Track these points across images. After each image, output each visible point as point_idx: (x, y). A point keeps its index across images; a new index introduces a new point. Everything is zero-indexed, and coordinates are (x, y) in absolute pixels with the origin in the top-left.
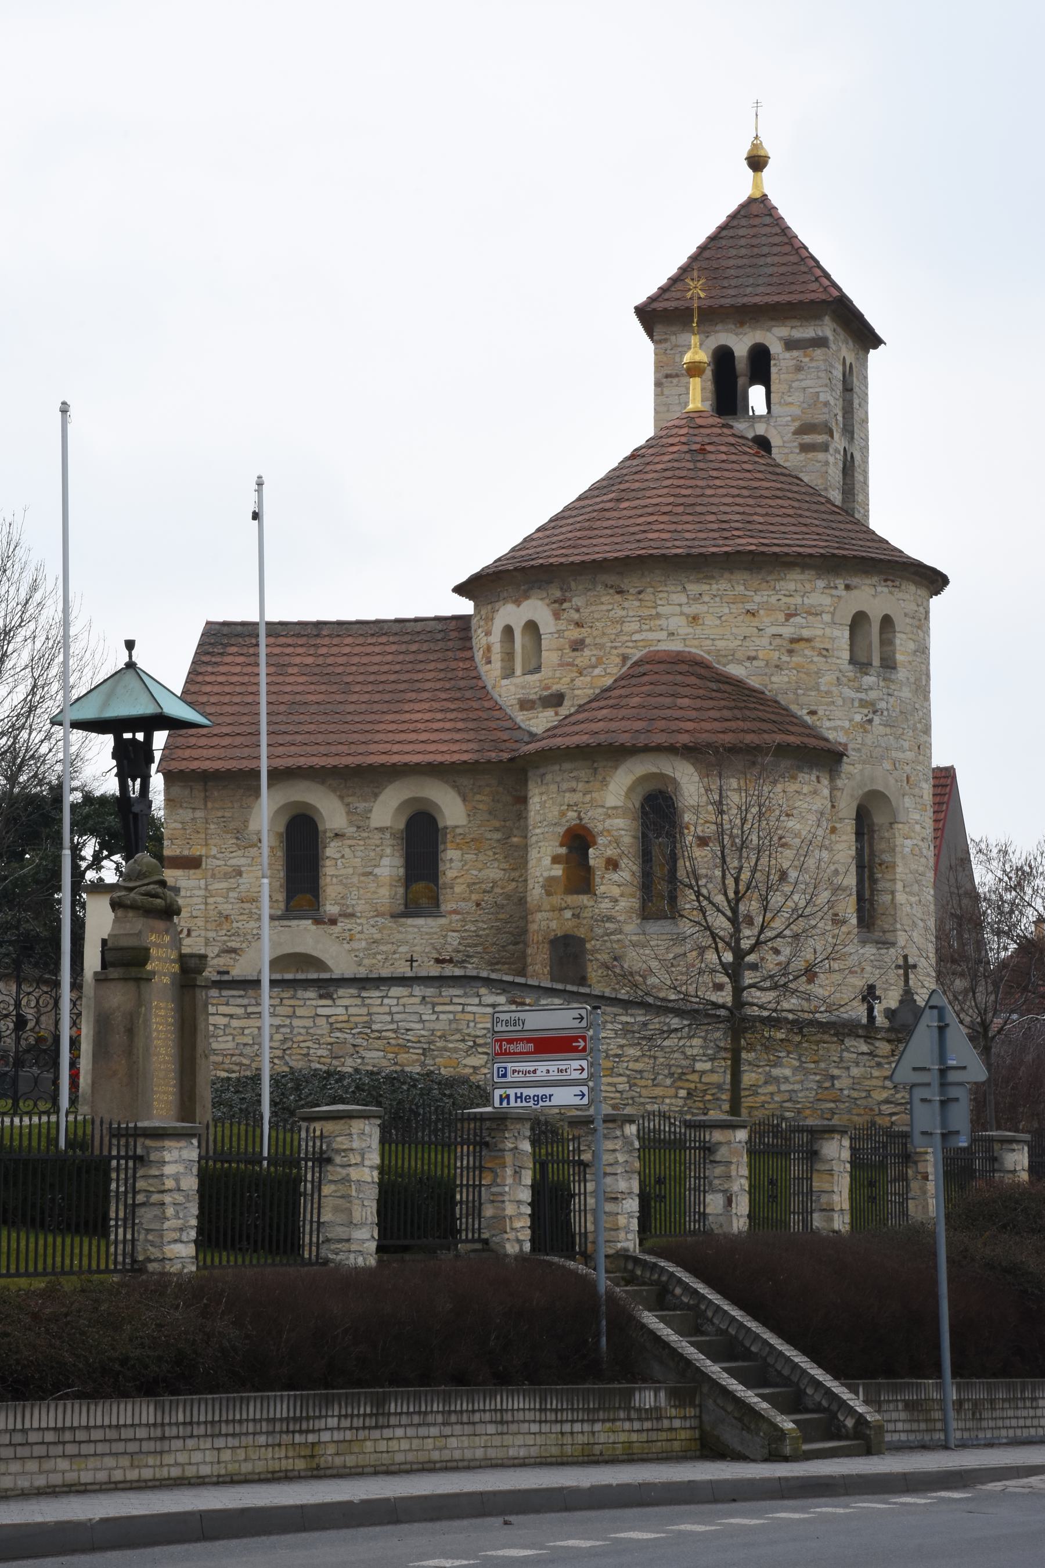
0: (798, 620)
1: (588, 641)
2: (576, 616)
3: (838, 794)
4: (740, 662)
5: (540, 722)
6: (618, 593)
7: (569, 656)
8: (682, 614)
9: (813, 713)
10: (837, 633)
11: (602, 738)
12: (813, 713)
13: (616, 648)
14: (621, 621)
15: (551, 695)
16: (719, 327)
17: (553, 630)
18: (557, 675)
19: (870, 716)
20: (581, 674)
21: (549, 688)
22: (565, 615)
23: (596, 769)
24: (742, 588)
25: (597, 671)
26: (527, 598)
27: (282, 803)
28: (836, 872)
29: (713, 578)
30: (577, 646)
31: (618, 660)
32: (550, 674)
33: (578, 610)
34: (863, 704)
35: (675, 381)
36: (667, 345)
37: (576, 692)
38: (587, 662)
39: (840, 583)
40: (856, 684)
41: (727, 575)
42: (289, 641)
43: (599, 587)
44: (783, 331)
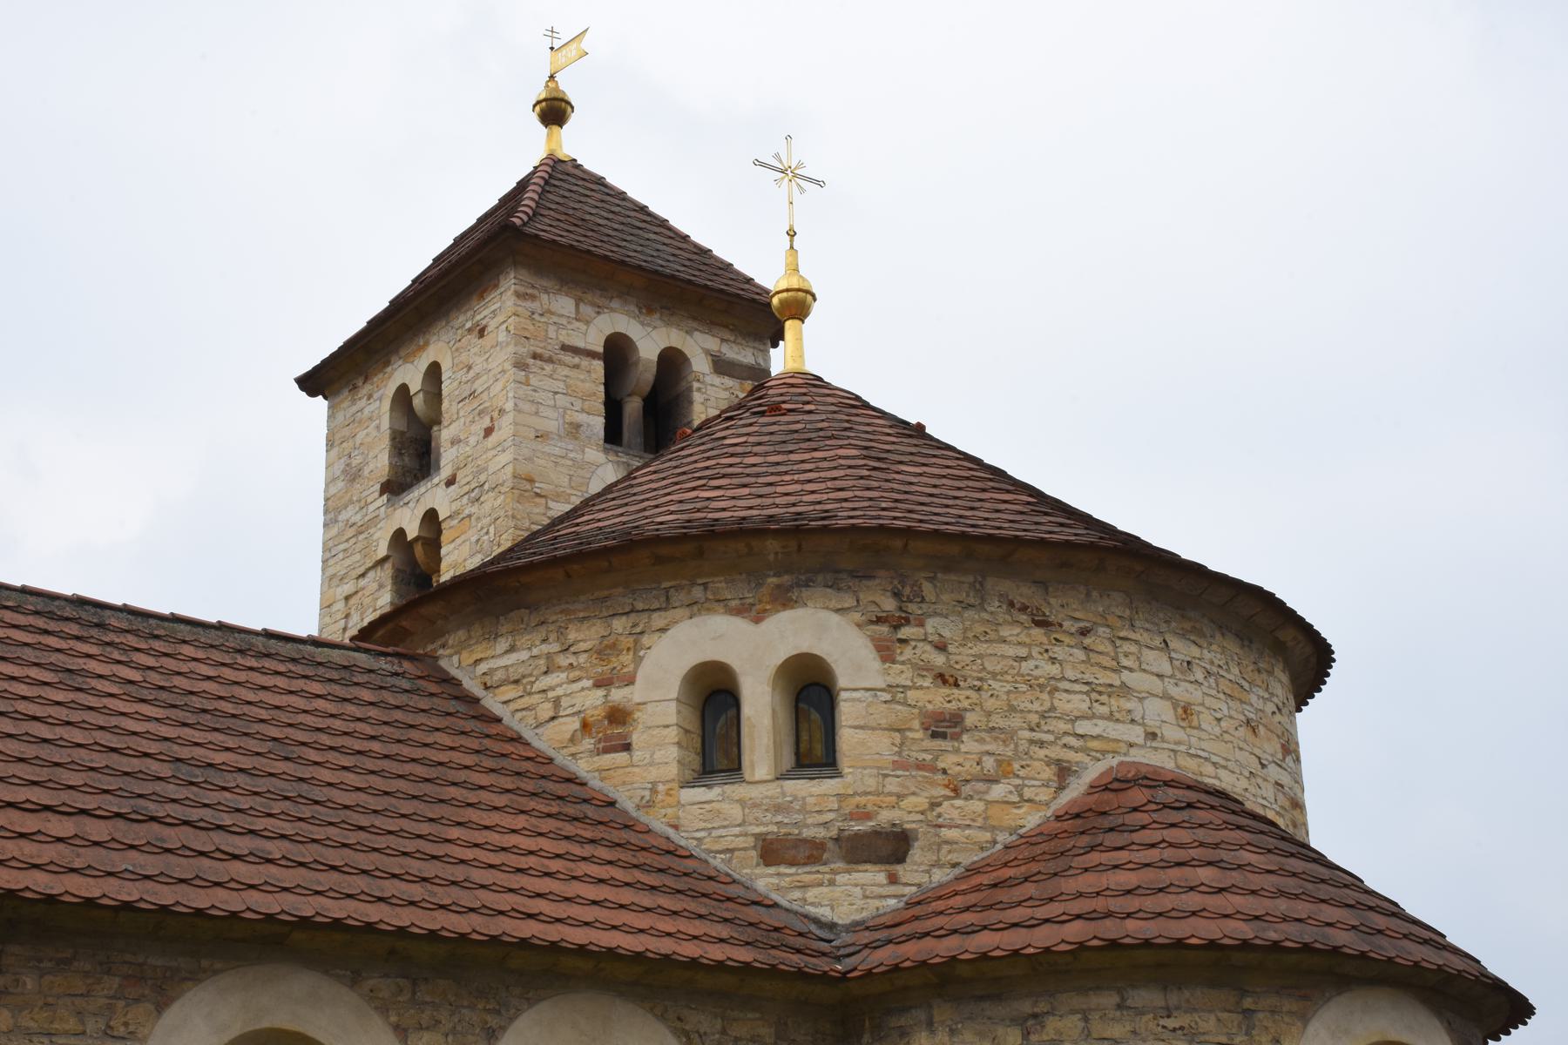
1: (970, 719)
2: (939, 660)
5: (847, 897)
6: (1038, 624)
7: (921, 746)
8: (1166, 696)
11: (1308, 934)
13: (1041, 744)
14: (1051, 687)
15: (876, 833)
16: (615, 304)
17: (880, 683)
18: (892, 785)
20: (957, 792)
21: (868, 816)
22: (908, 653)
23: (1247, 1013)
24: (1235, 670)
25: (998, 791)
26: (784, 599)
27: (235, 1031)
29: (1204, 636)
30: (944, 727)
31: (1048, 773)
32: (871, 783)
33: (941, 647)
35: (548, 368)
36: (535, 305)
37: (947, 833)
38: (970, 767)
41: (1218, 636)
42: (40, 622)
43: (994, 605)
44: (712, 343)
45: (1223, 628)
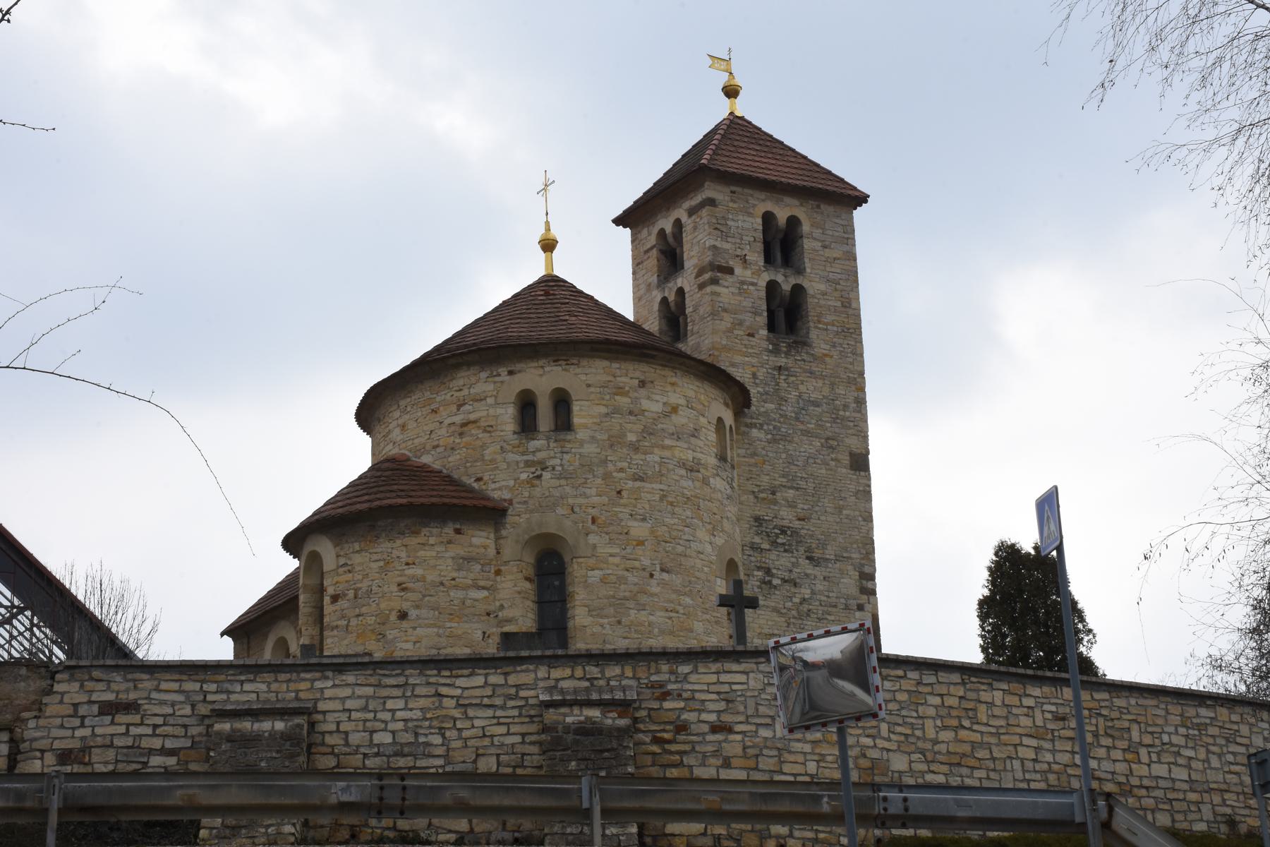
0: (467, 407)
3: (501, 541)
4: (428, 452)
9: (479, 480)
10: (500, 411)
12: (479, 480)
19: (538, 473)
28: (502, 607)
34: (528, 464)
39: (503, 371)
40: (521, 449)
45: (422, 382)
